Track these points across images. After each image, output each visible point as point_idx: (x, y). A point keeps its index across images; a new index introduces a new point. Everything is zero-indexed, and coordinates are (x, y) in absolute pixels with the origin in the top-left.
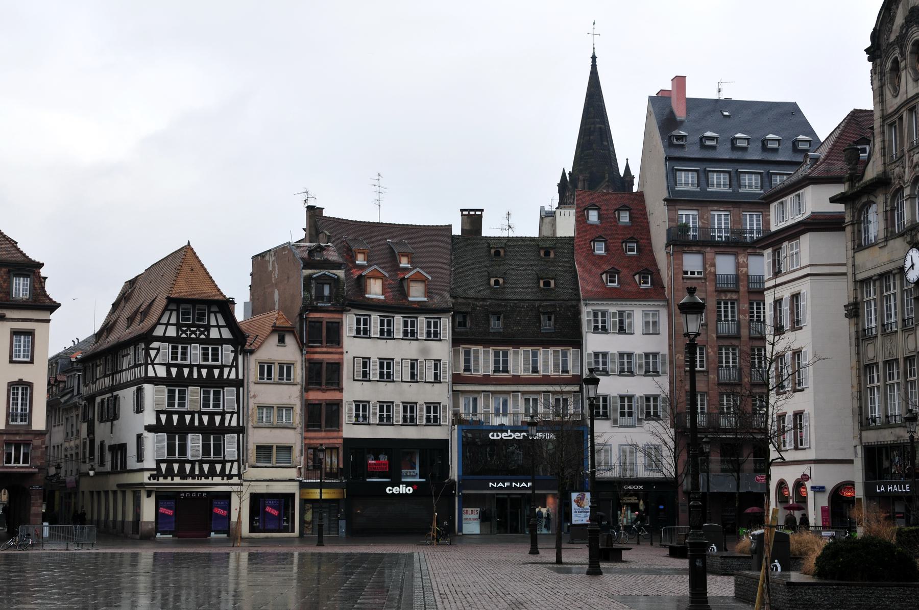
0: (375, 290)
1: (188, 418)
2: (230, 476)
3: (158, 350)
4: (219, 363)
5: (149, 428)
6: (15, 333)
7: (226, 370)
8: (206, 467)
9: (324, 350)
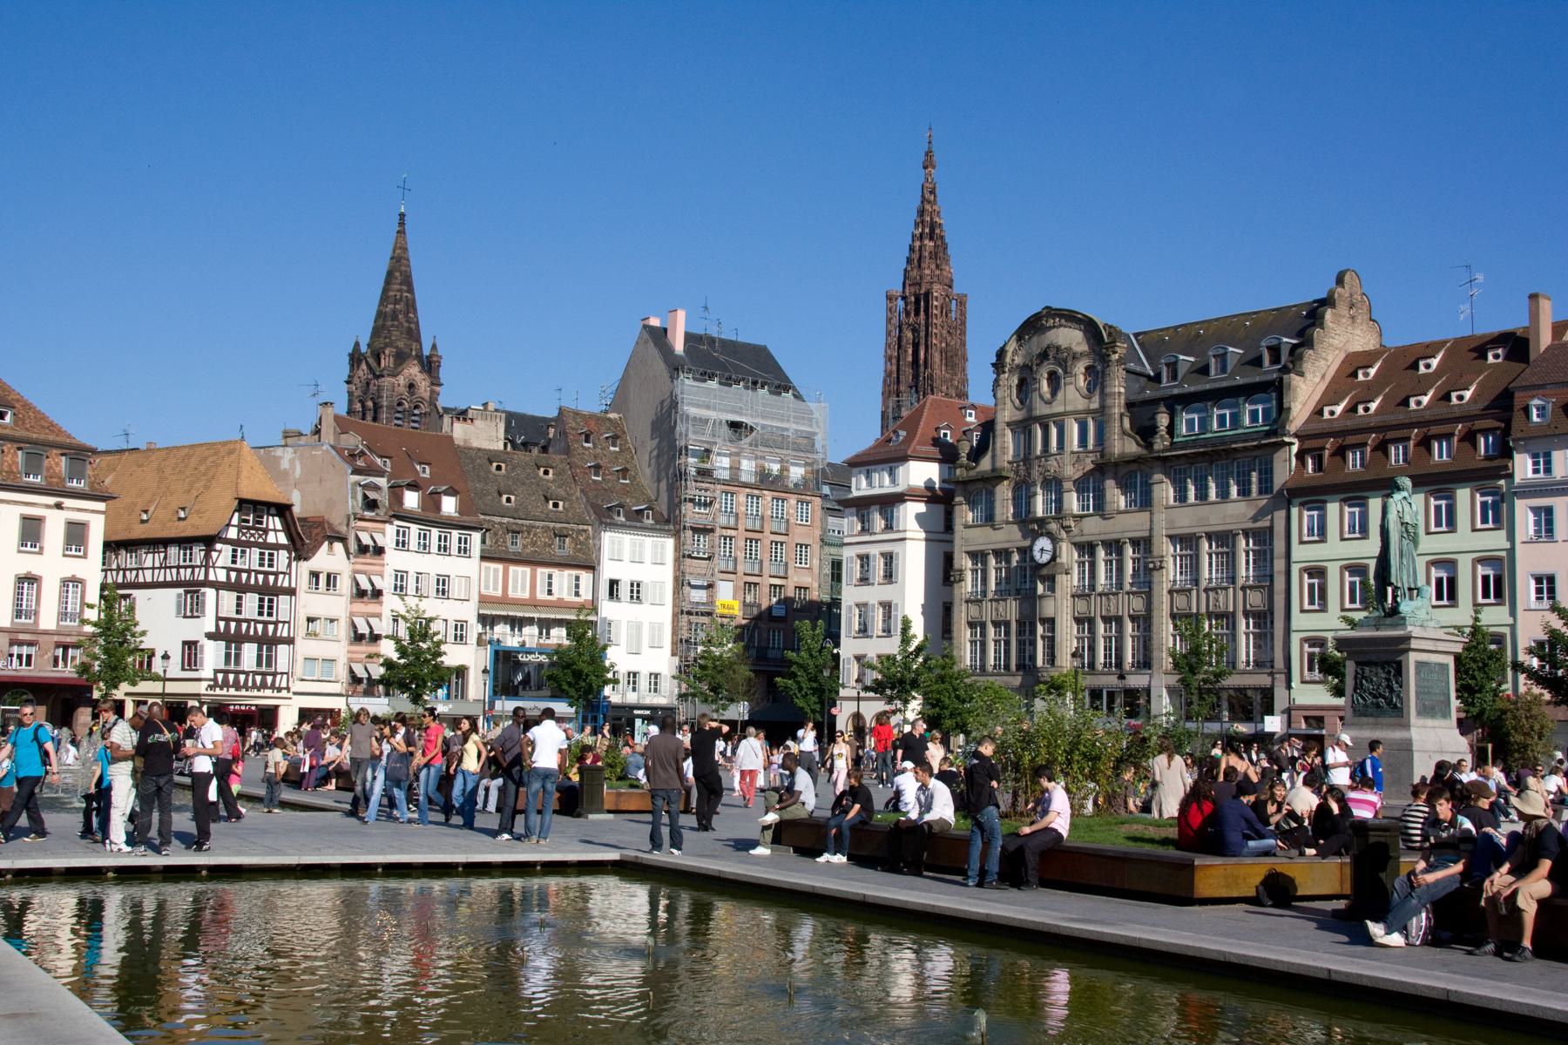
0: (411, 500)
1: (244, 626)
2: (280, 689)
3: (220, 551)
4: (274, 569)
5: (210, 636)
6: (71, 525)
7: (281, 576)
8: (258, 678)
9: (369, 561)
